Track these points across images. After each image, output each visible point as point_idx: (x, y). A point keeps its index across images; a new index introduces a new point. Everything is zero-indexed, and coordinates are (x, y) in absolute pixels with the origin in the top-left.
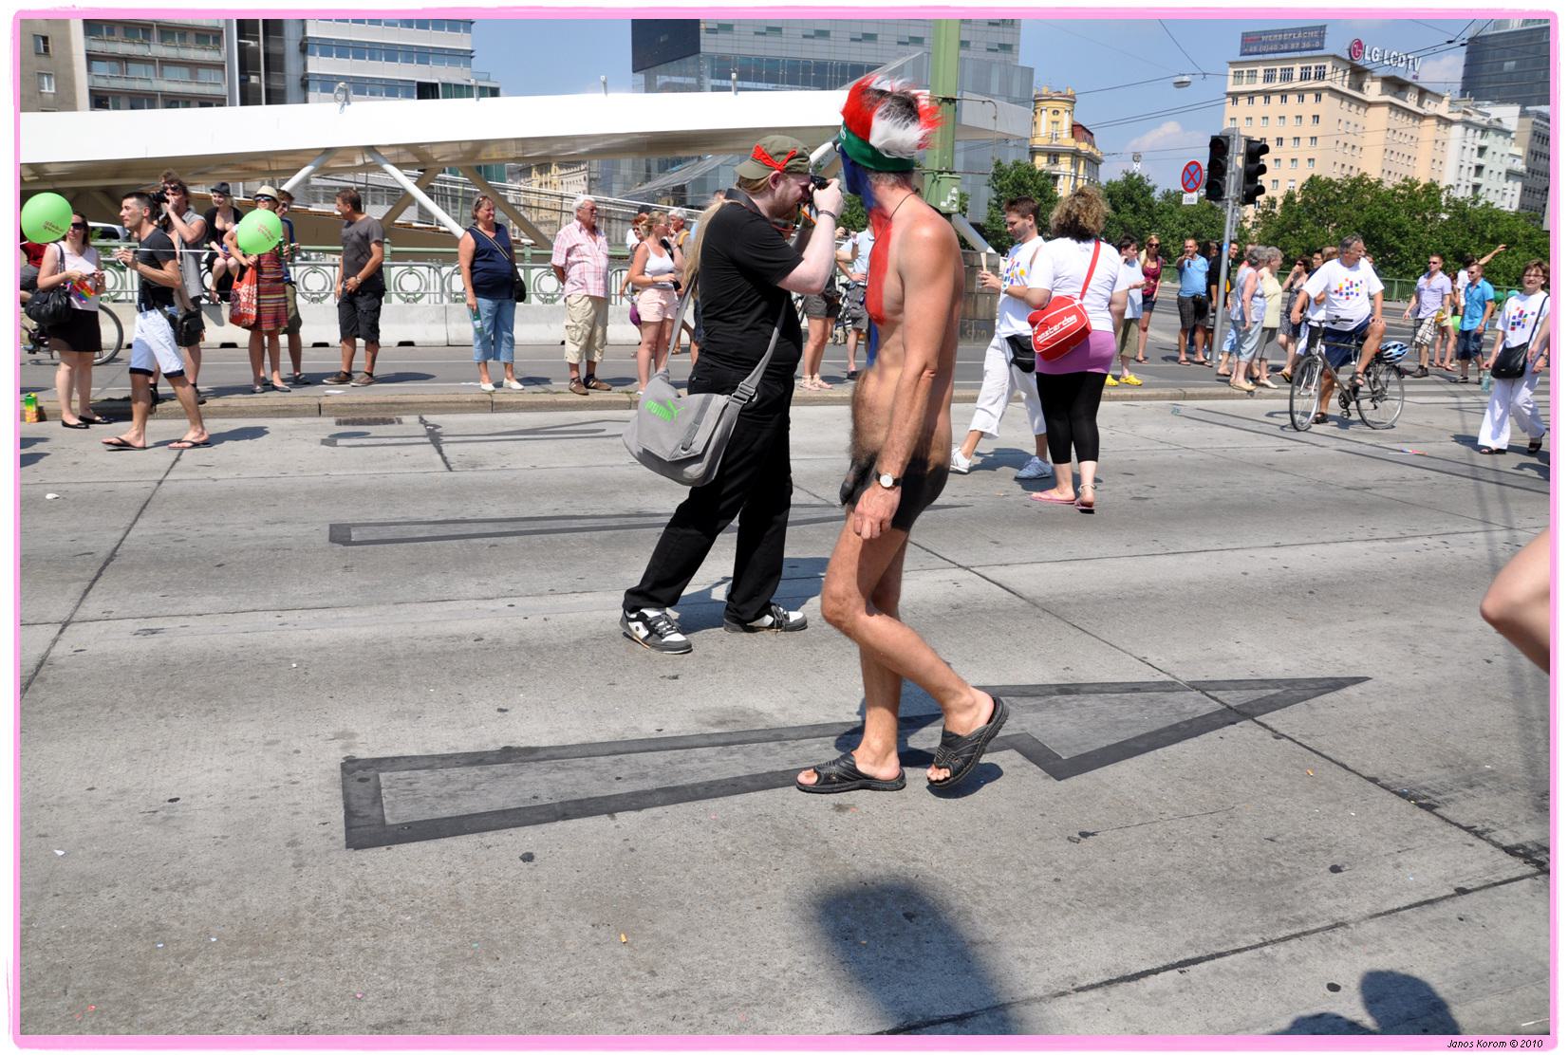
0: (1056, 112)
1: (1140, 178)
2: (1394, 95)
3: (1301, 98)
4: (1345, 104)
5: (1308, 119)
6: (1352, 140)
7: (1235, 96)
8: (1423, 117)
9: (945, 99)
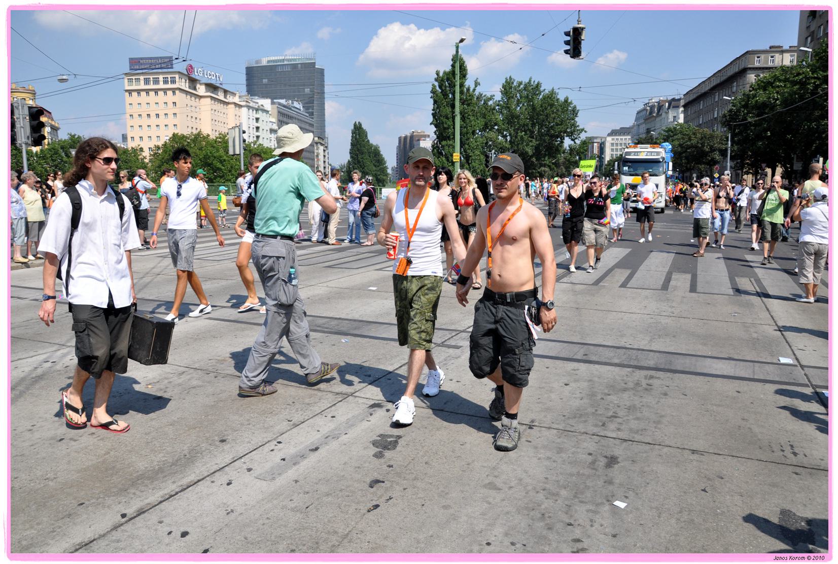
1: (79, 137)
3: (165, 93)
4: (189, 97)
5: (170, 105)
6: (195, 115)
7: (130, 92)
8: (228, 103)
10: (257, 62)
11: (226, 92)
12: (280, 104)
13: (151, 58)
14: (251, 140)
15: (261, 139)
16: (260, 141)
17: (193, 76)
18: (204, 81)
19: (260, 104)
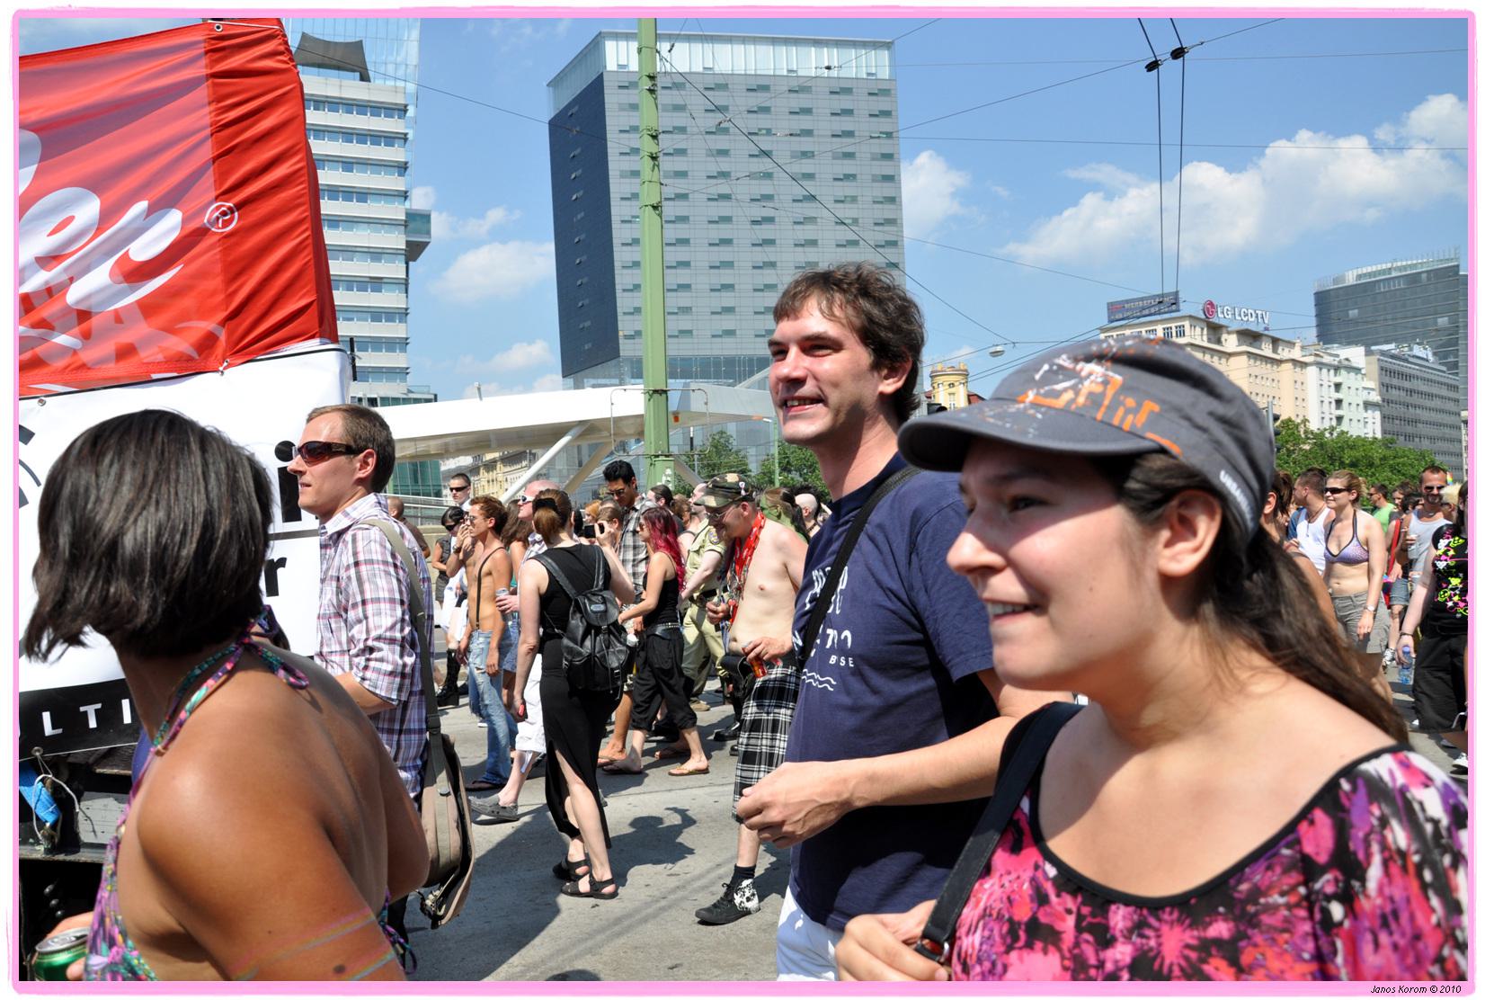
0: (952, 385)
2: (1251, 345)
8: (1279, 362)
9: (655, 391)
10: (1335, 281)
11: (1275, 342)
12: (1383, 353)
13: (1142, 299)
14: (1327, 425)
15: (1345, 421)
16: (1345, 427)
17: (1214, 320)
18: (1235, 326)
19: (1342, 357)
